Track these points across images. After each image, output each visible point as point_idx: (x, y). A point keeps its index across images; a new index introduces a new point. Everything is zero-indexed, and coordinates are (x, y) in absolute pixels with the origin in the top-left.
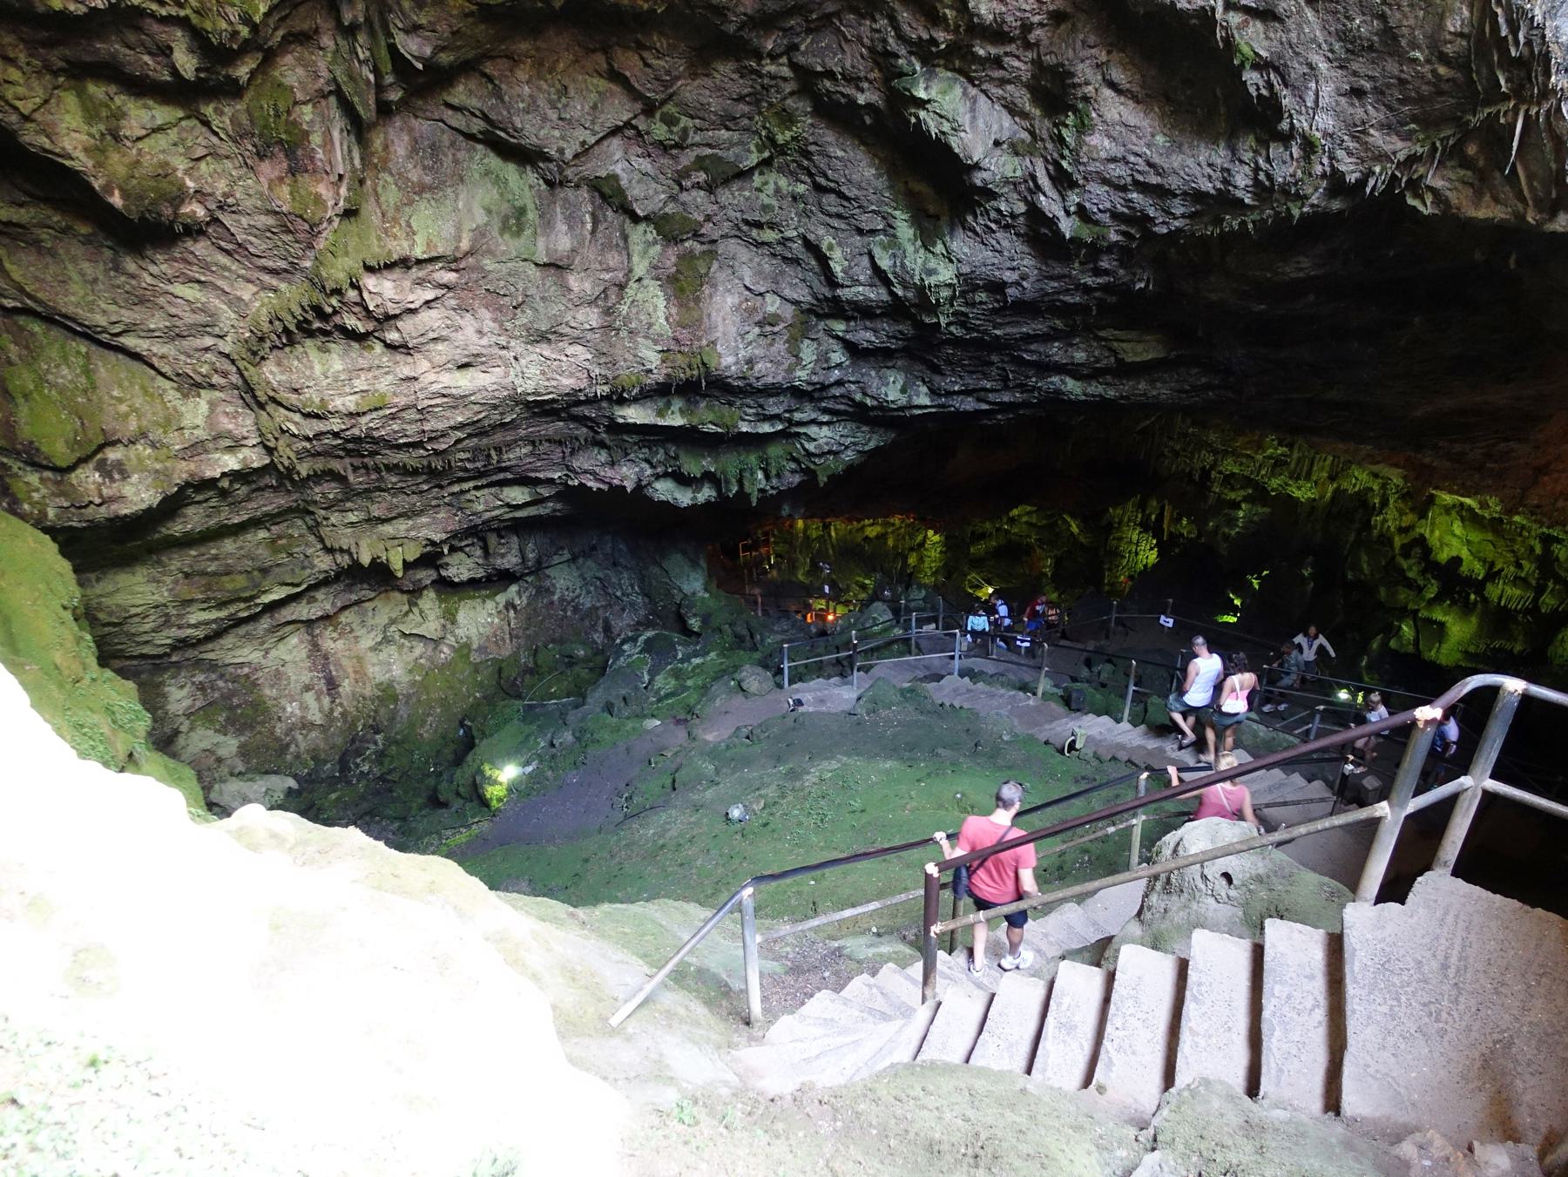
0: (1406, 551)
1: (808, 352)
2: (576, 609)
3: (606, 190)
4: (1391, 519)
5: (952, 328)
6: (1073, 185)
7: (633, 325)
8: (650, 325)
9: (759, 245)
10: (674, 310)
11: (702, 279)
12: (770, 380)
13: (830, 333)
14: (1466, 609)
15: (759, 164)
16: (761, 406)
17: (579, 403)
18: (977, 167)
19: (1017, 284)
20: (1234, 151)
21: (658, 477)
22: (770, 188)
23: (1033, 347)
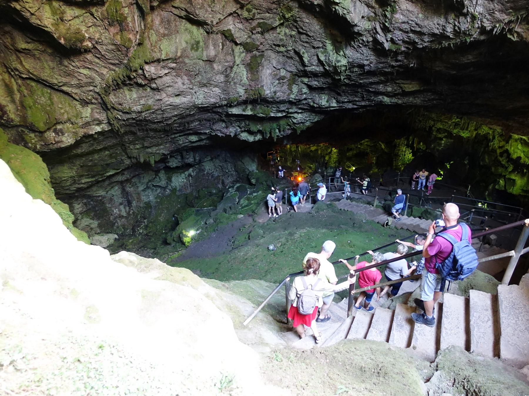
0: (501, 155)
1: (295, 89)
3: (227, 35)
4: (496, 143)
5: (345, 80)
6: (389, 31)
7: (235, 81)
8: (241, 80)
9: (278, 52)
10: (249, 75)
11: (259, 64)
12: (282, 98)
13: (302, 82)
15: (279, 25)
16: (278, 107)
17: (216, 107)
18: (356, 25)
19: (369, 65)
21: (242, 132)
22: (283, 33)
23: (373, 86)
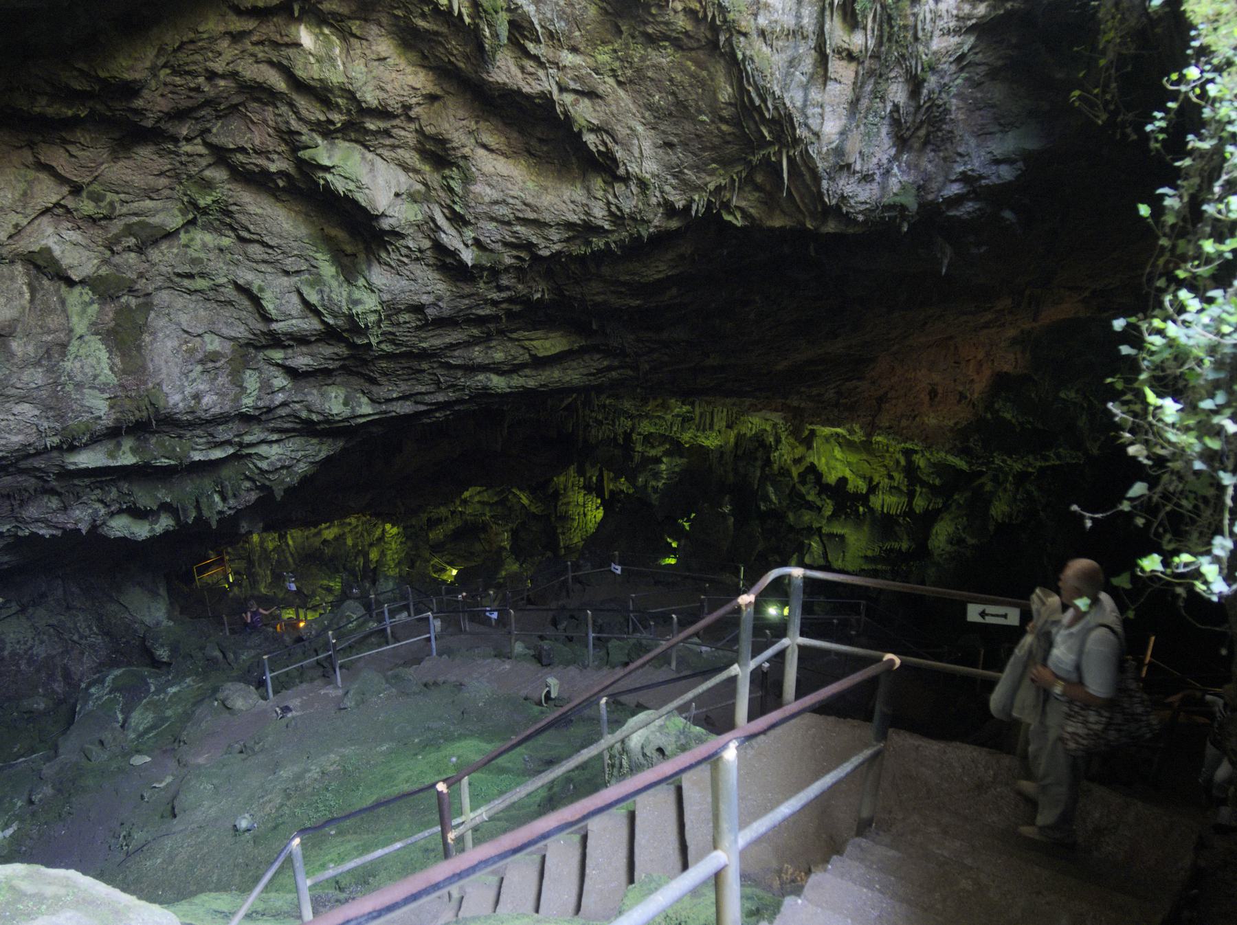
0: (803, 481)
1: (251, 381)
2: (31, 661)
3: (40, 262)
4: (785, 453)
5: (383, 346)
6: (466, 223)
7: (78, 379)
8: (96, 377)
9: (191, 292)
10: (117, 361)
11: (141, 329)
12: (217, 410)
13: (269, 361)
14: (858, 520)
15: (183, 226)
16: (211, 435)
17: (28, 456)
18: (383, 215)
19: (434, 304)
20: (588, 190)
21: (112, 515)
22: (198, 241)
23: (456, 353)
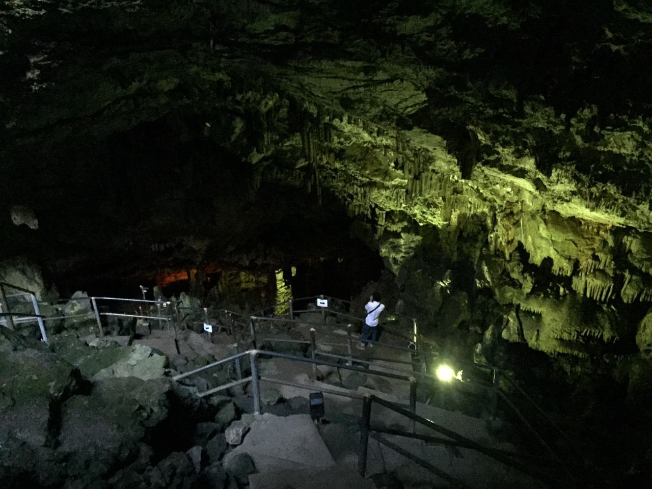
14: (558, 301)
